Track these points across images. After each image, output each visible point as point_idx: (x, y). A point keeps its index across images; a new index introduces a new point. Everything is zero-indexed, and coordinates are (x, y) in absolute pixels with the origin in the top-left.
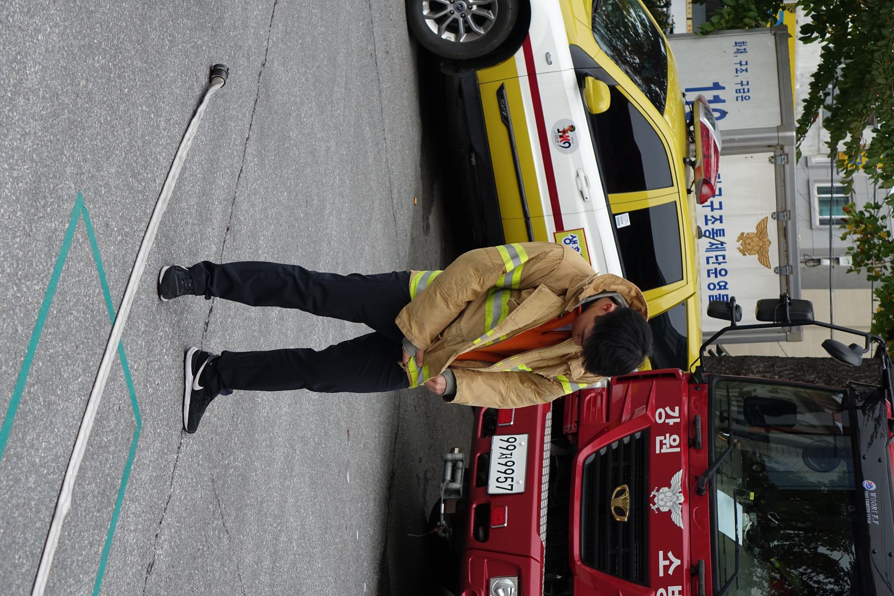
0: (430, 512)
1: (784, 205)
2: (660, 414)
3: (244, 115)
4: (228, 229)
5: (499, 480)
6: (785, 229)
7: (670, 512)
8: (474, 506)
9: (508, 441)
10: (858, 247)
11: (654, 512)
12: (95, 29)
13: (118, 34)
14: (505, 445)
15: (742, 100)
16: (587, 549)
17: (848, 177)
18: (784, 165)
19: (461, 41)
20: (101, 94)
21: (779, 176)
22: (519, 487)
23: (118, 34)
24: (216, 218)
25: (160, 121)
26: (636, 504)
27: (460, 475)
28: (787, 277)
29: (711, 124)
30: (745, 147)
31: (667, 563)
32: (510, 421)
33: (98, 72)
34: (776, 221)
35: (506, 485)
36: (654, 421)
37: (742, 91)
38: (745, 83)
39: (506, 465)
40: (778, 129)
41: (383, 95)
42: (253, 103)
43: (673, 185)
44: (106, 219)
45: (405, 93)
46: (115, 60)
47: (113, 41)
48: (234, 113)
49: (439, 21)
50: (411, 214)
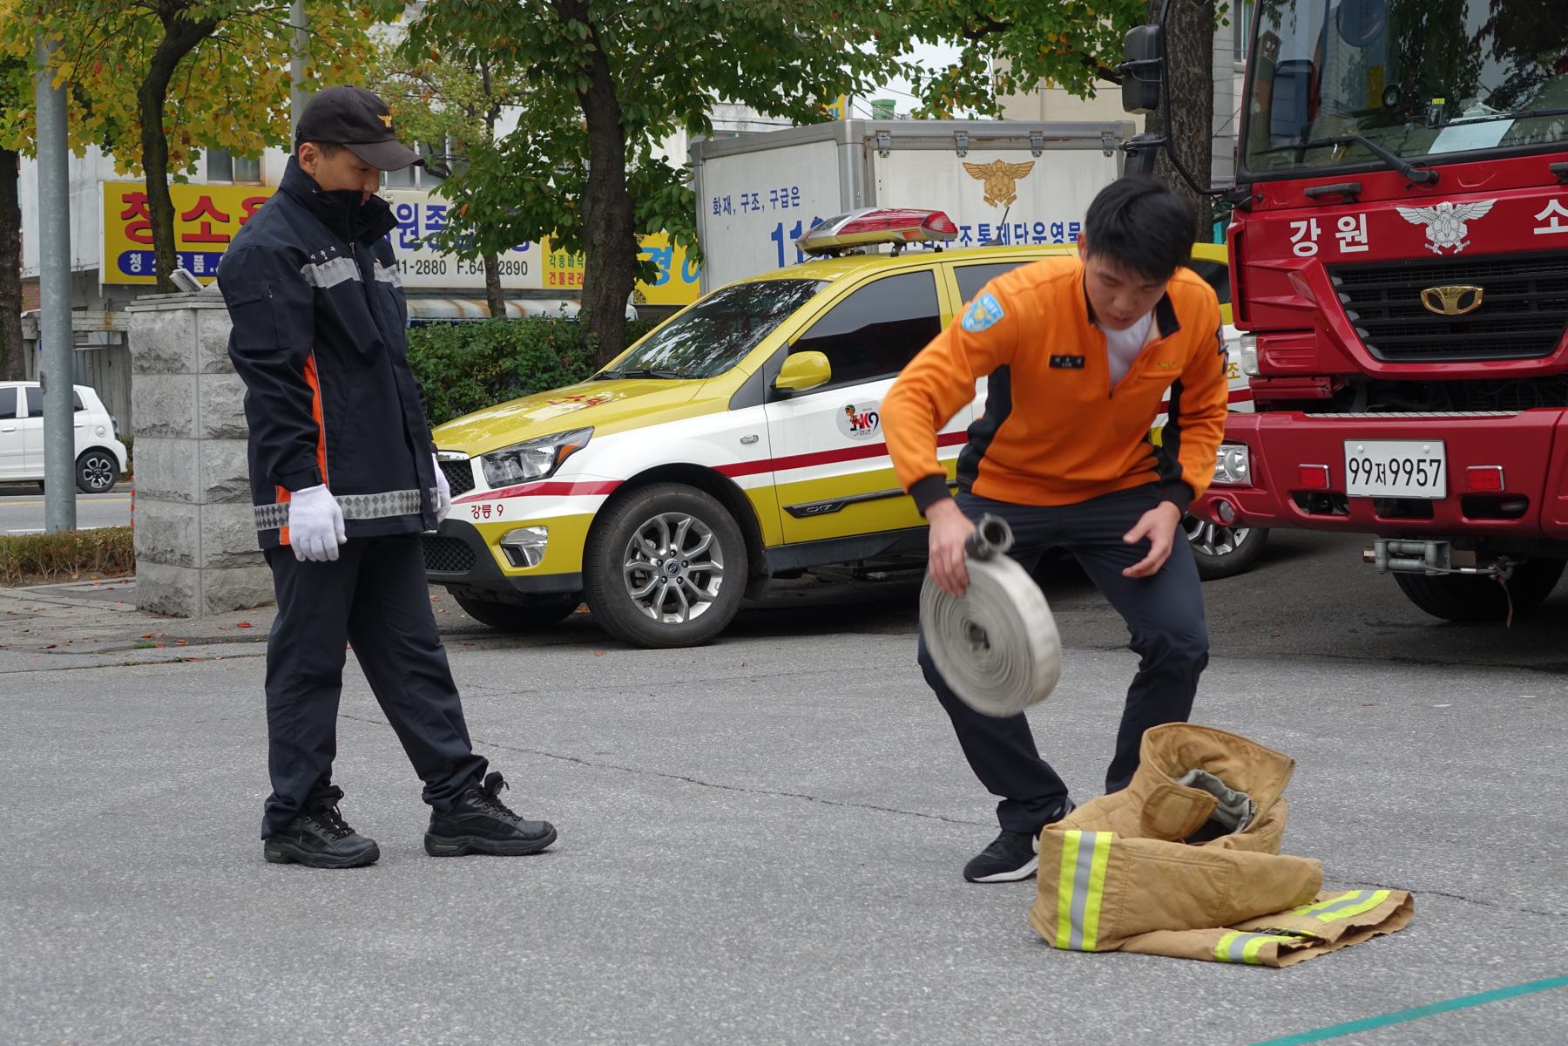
0: (1431, 617)
1: (947, 139)
2: (1302, 249)
3: (906, 822)
5: (1422, 481)
6: (980, 139)
7: (1468, 222)
8: (1465, 520)
9: (1356, 472)
10: (970, 107)
11: (1468, 246)
12: (822, 1038)
13: (820, 1001)
14: (1362, 475)
17: (900, 70)
19: (721, 567)
20: (949, 1030)
21: (907, 145)
22: (1436, 449)
26: (1453, 277)
27: (1411, 546)
28: (1046, 139)
29: (835, 224)
31: (1554, 220)
33: (907, 1037)
34: (969, 152)
36: (1315, 259)
37: (785, 199)
38: (773, 196)
39: (1396, 473)
40: (841, 143)
42: (879, 811)
43: (931, 271)
44: (1199, 1027)
46: (873, 1007)
47: (837, 1010)
48: (906, 836)
49: (693, 601)
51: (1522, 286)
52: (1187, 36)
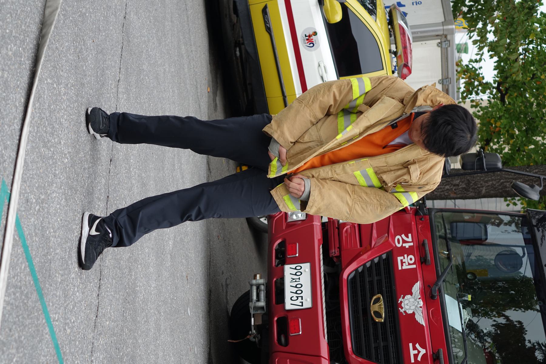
0: (231, 308)
1: (447, 75)
2: (398, 240)
3: (116, 62)
4: (111, 161)
5: (293, 299)
7: (414, 314)
8: (276, 319)
9: (295, 269)
10: (464, 87)
11: (403, 314)
12: (6, 19)
13: (25, 19)
14: (294, 272)
15: (416, 4)
16: (356, 343)
17: (480, 51)
18: (447, 48)
20: (15, 79)
21: (443, 55)
22: (308, 304)
23: (25, 19)
24: (103, 156)
25: (61, 88)
26: (388, 308)
27: (262, 295)
29: (404, 23)
30: (421, 37)
31: (416, 352)
32: (296, 254)
33: (10, 59)
35: (298, 302)
36: (394, 246)
39: (296, 287)
40: (443, 24)
41: (189, 19)
42: (121, 50)
43: (383, 69)
44: (26, 195)
45: (199, 15)
46: (24, 44)
47: (21, 27)
48: (109, 62)
50: (207, 100)
51: (385, 339)
52: (500, 185)
